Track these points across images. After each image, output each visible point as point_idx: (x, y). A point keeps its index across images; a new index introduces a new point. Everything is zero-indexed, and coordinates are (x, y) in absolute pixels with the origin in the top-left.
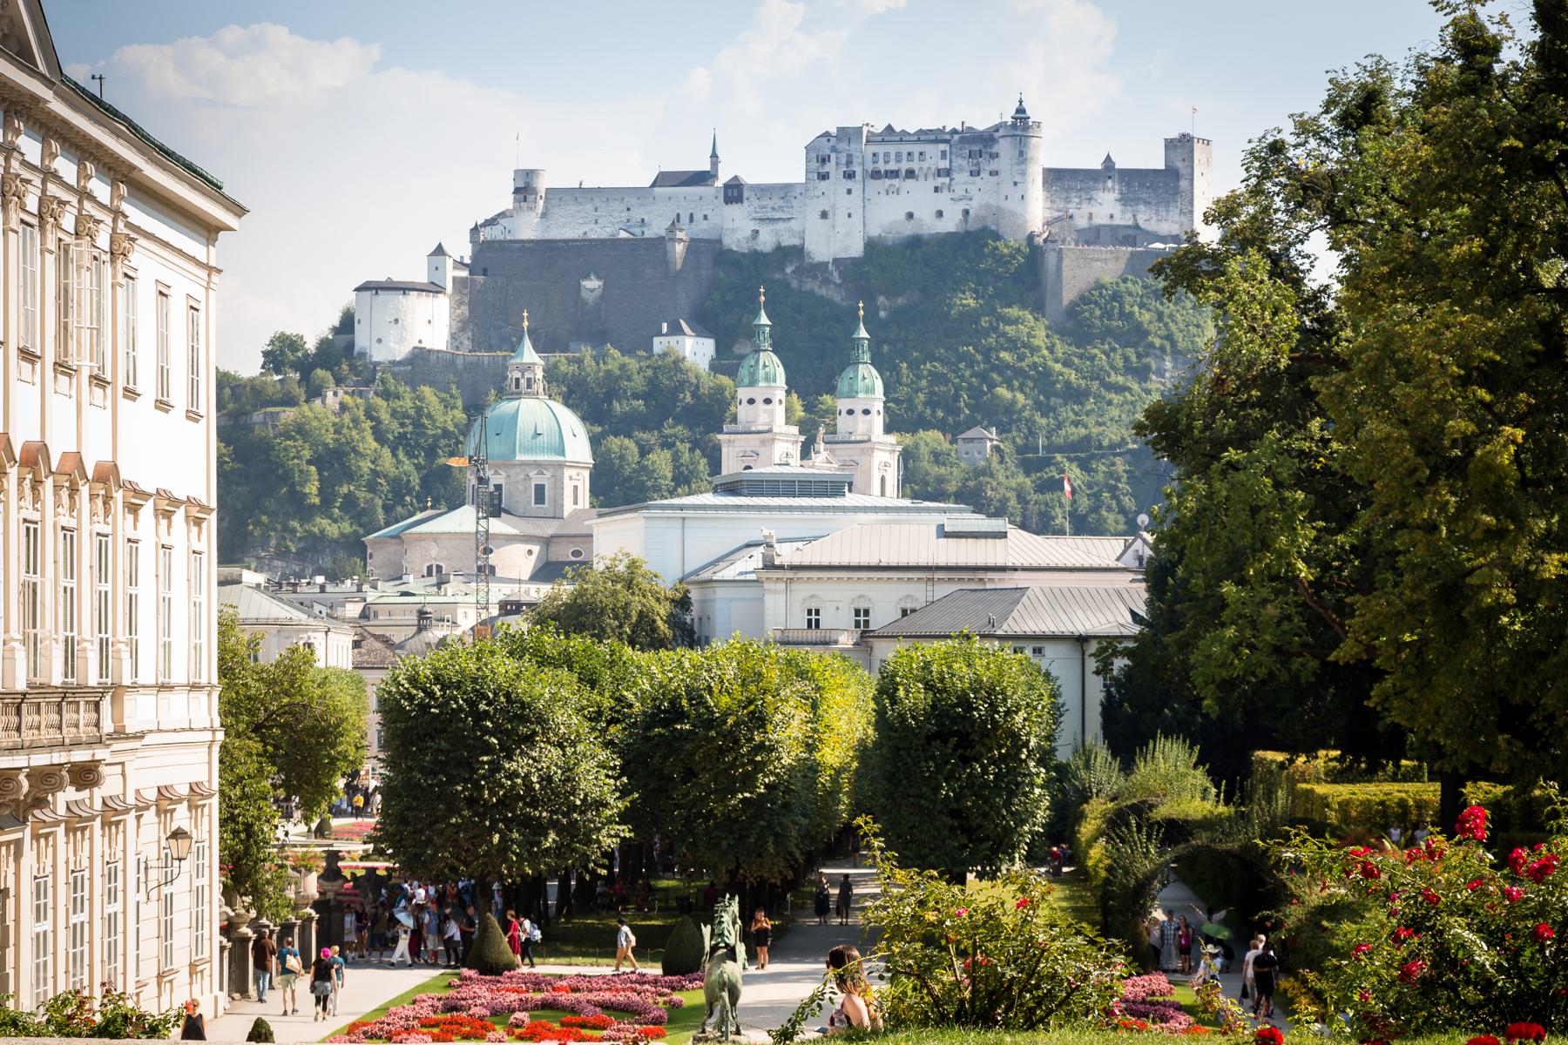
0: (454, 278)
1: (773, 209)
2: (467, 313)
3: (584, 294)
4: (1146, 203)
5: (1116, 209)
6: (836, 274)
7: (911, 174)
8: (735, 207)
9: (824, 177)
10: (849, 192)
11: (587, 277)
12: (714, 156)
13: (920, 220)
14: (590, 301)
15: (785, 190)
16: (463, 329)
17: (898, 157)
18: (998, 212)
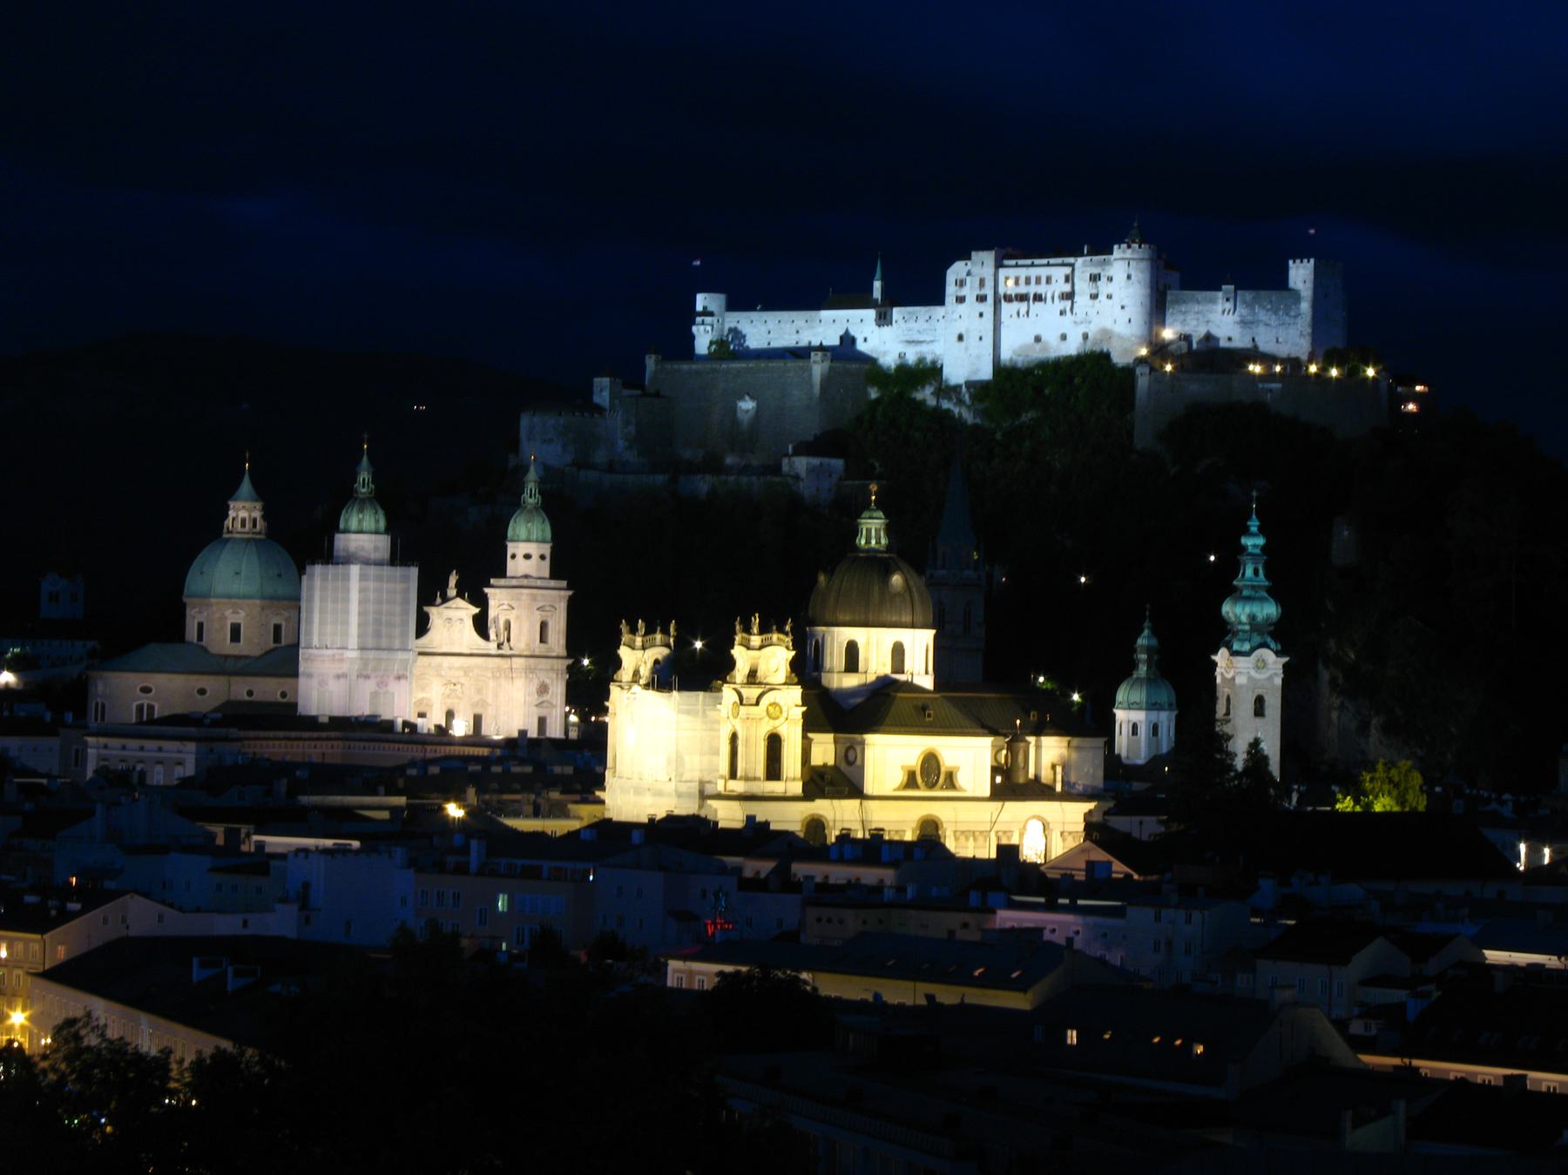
1: (919, 331)
3: (739, 415)
4: (1267, 325)
6: (967, 397)
7: (1038, 298)
9: (961, 300)
10: (981, 315)
11: (742, 398)
17: (1028, 281)
18: (1106, 334)
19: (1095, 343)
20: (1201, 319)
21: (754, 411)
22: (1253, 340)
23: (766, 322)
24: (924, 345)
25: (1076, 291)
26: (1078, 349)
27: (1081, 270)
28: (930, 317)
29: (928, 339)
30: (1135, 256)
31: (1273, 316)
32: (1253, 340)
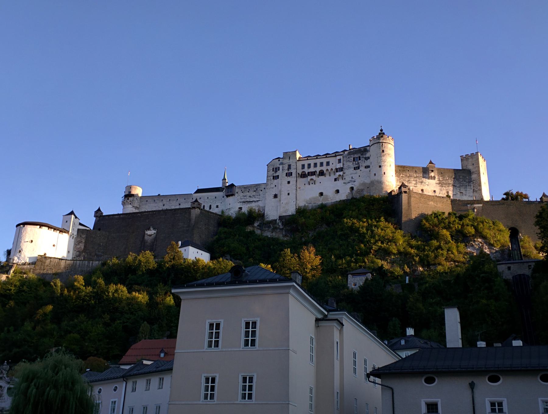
0: (78, 230)
1: (250, 197)
2: (83, 247)
3: (146, 237)
5: (437, 189)
6: (280, 224)
7: (322, 173)
8: (231, 198)
10: (289, 182)
11: (149, 229)
12: (224, 179)
13: (327, 196)
14: (149, 241)
15: (256, 188)
16: (79, 256)
17: (315, 165)
19: (360, 191)
20: (418, 180)
21: (155, 235)
22: (448, 192)
23: (162, 200)
24: (254, 203)
25: (344, 168)
26: (347, 195)
27: (347, 157)
28: (257, 189)
29: (255, 200)
30: (385, 141)
31: (457, 182)
32: (448, 192)
